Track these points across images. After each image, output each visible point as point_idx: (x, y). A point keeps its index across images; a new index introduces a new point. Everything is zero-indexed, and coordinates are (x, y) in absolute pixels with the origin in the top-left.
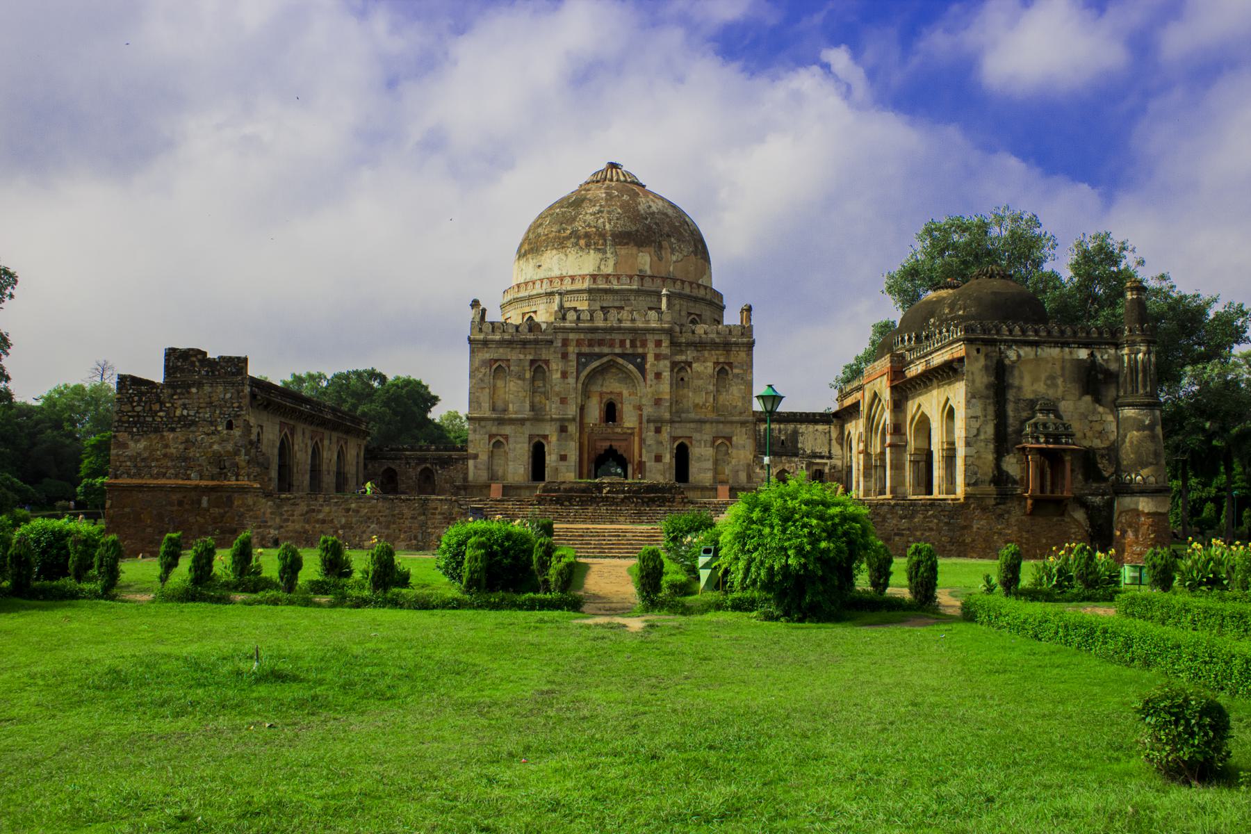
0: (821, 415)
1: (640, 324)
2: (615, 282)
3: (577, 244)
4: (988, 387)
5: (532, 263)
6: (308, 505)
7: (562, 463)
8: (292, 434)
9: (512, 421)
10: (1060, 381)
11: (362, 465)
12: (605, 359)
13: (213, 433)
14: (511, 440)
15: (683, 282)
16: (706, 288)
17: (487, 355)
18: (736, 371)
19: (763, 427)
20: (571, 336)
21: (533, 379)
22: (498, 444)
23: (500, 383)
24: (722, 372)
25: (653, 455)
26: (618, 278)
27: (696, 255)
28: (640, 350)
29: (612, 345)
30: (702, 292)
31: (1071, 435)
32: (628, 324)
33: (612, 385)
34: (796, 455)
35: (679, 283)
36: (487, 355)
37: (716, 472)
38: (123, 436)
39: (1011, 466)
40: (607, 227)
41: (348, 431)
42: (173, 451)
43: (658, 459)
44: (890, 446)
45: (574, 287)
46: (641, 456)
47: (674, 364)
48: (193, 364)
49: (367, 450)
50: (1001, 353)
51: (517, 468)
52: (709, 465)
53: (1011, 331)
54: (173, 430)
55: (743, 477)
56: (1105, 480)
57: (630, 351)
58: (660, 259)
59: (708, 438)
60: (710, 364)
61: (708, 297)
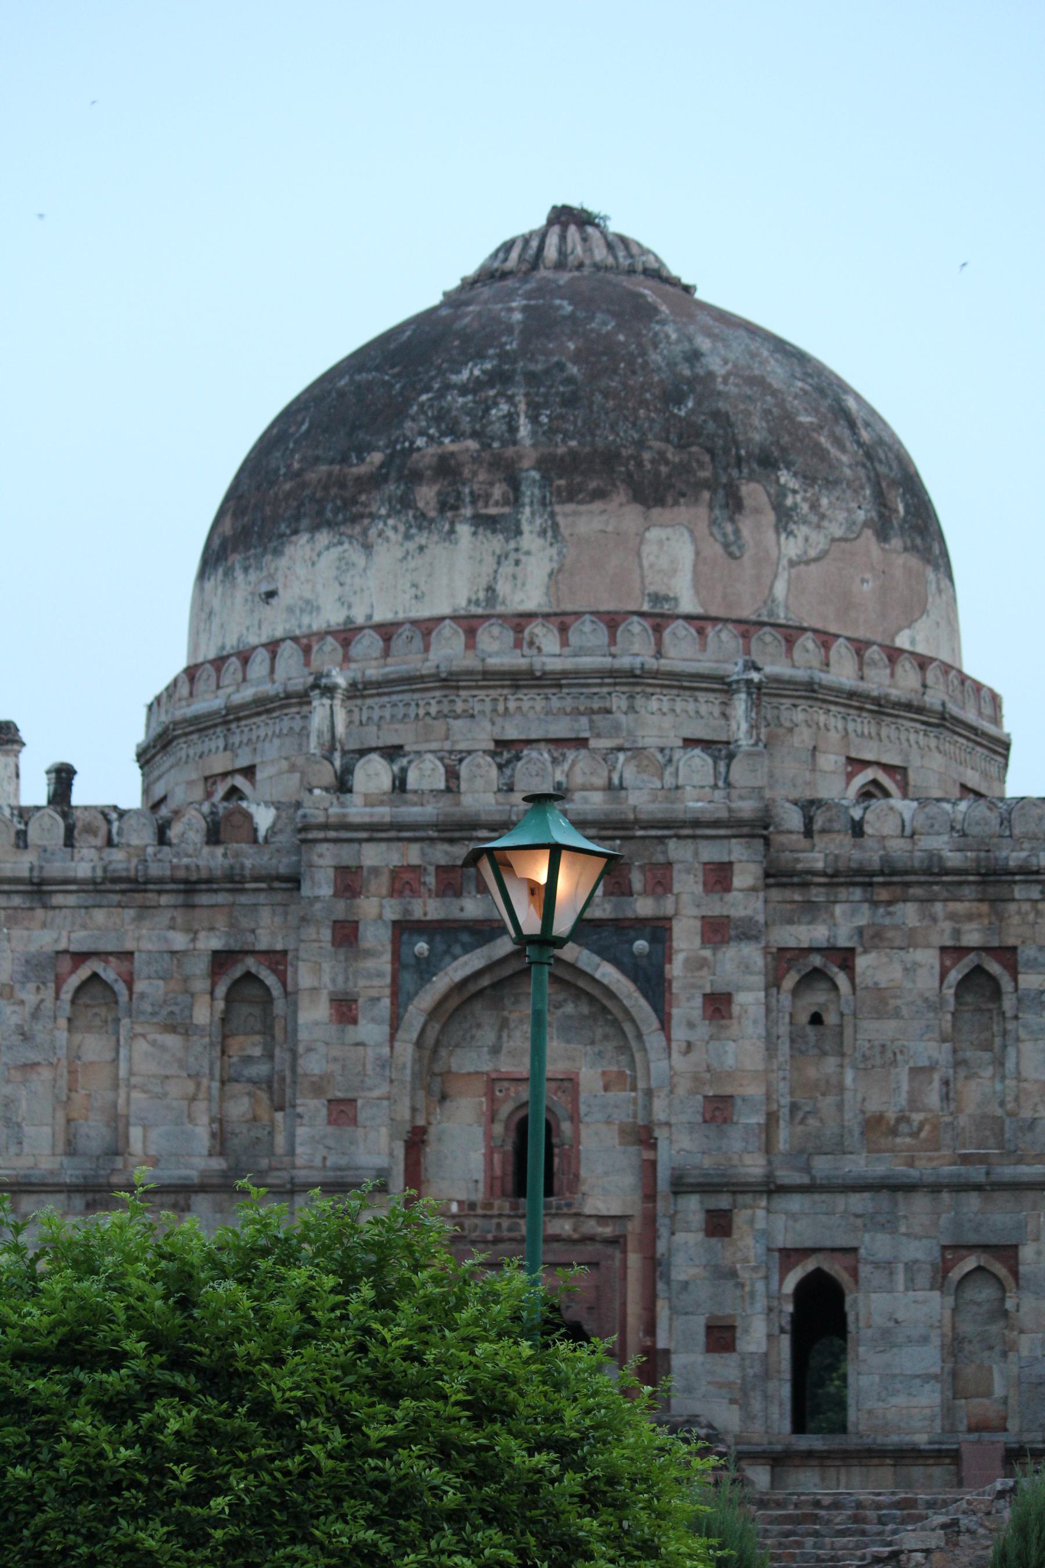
1: (641, 798)
3: (406, 502)
15: (826, 639)
16: (923, 663)
18: (1029, 981)
20: (372, 855)
23: (94, 1046)
25: (698, 1324)
26: (562, 622)
27: (883, 534)
28: (644, 907)
30: (905, 683)
35: (807, 641)
37: (956, 1384)
40: (524, 430)
43: (721, 1337)
45: (395, 667)
46: (650, 1328)
47: (782, 959)
52: (928, 1358)
58: (732, 549)
59: (920, 1251)
60: (928, 958)
61: (933, 699)
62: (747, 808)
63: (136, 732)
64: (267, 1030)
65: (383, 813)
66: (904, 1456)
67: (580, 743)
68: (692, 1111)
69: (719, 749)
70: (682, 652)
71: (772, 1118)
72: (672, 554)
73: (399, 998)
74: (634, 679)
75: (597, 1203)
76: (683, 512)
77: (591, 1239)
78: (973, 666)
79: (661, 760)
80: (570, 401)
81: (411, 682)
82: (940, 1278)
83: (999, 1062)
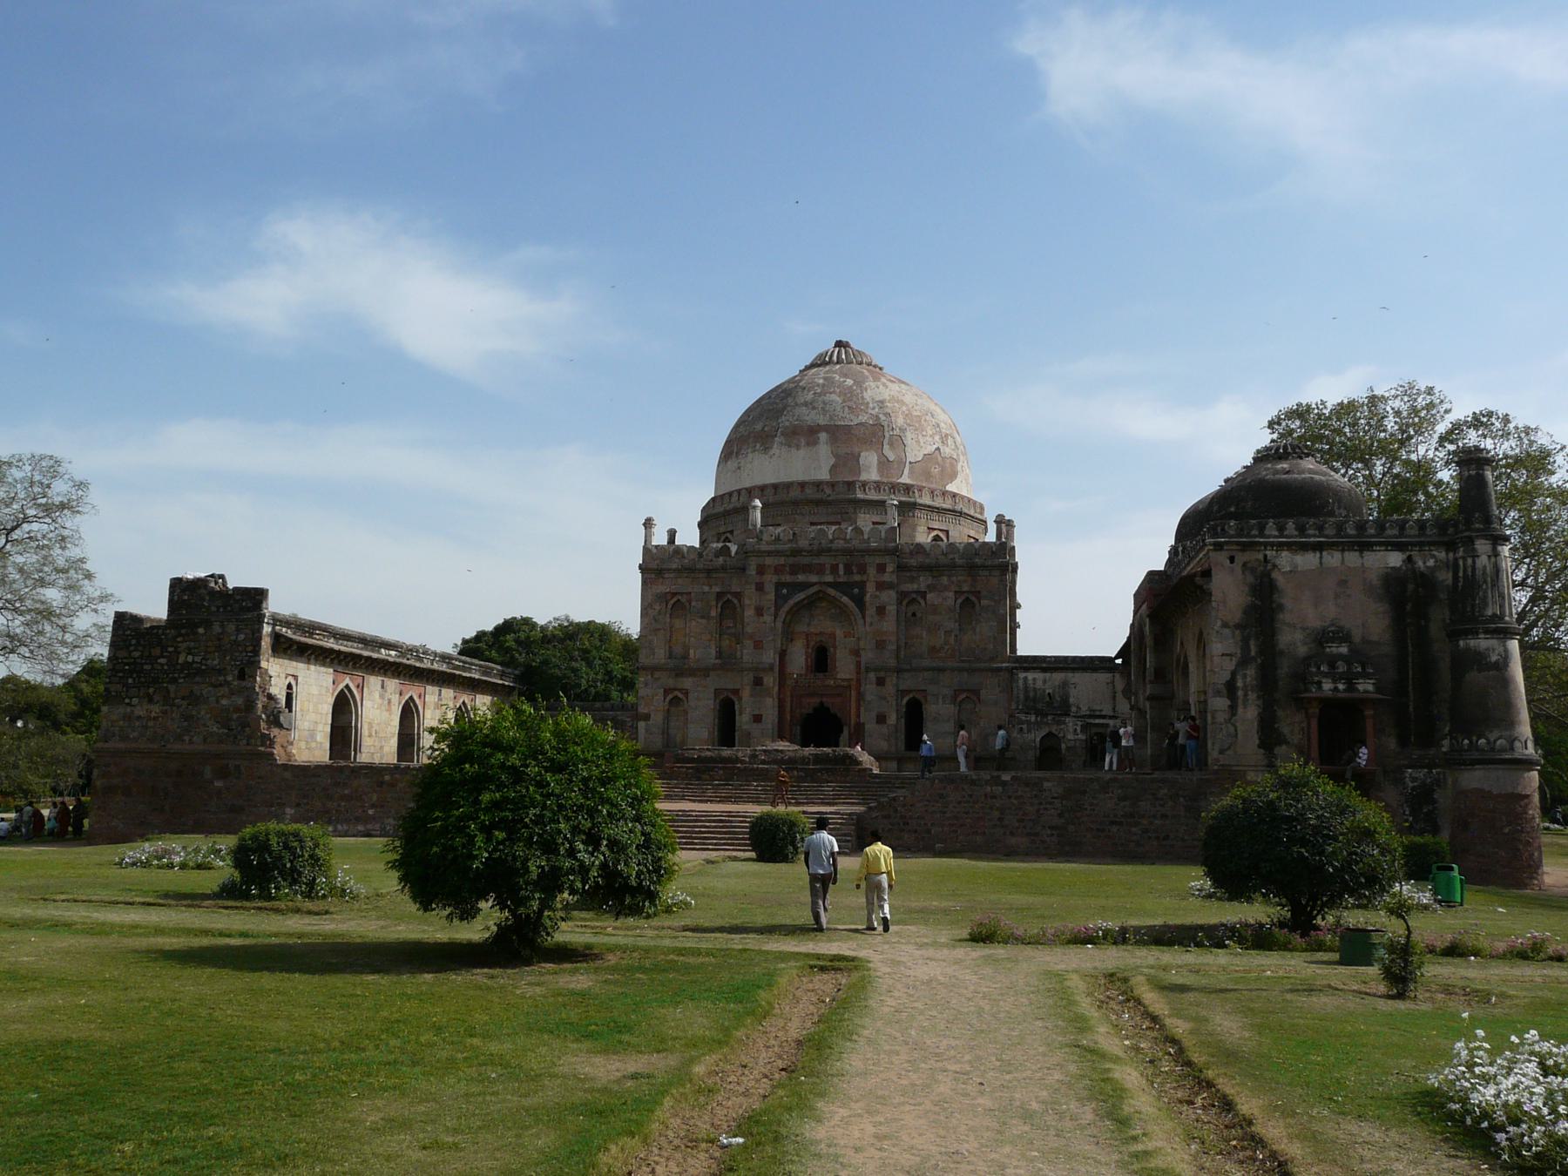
2: (828, 491)
8: (361, 687)
9: (692, 672)
16: (954, 495)
17: (662, 588)
18: (984, 602)
19: (1022, 675)
20: (769, 561)
22: (675, 701)
23: (678, 623)
24: (968, 606)
25: (874, 715)
28: (857, 578)
29: (820, 570)
32: (840, 544)
33: (822, 624)
43: (881, 719)
44: (1151, 698)
47: (903, 595)
53: (1281, 529)
54: (174, 681)
60: (951, 594)
61: (958, 508)
65: (772, 548)
70: (872, 496)
71: (898, 648)
73: (777, 608)
75: (841, 675)
81: (783, 503)
82: (954, 700)
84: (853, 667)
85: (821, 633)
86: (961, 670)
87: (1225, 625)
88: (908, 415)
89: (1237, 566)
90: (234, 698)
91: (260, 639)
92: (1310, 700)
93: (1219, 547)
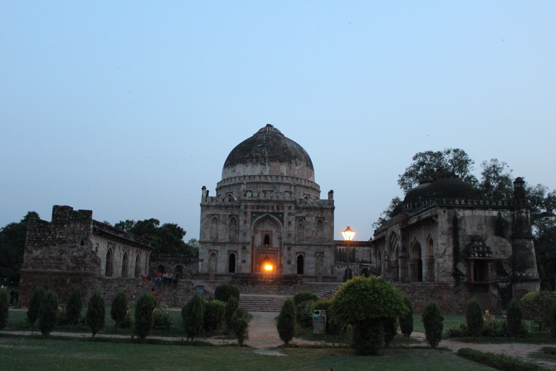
0: (366, 242)
1: (281, 198)
2: (269, 179)
3: (251, 161)
4: (449, 229)
5: (231, 170)
6: (119, 283)
7: (244, 264)
8: (114, 248)
9: (220, 244)
10: (484, 226)
11: (148, 263)
12: (264, 215)
13: (74, 247)
14: (219, 253)
15: (301, 179)
16: (312, 182)
17: (209, 212)
18: (326, 221)
19: (338, 248)
20: (249, 204)
21: (231, 224)
22: (213, 254)
23: (215, 226)
24: (320, 222)
25: (286, 261)
26: (271, 176)
28: (281, 211)
30: (310, 184)
31: (491, 253)
32: (275, 199)
33: (267, 227)
34: (354, 261)
36: (209, 212)
37: (316, 268)
38: (29, 248)
39: (462, 267)
41: (142, 247)
42: (54, 255)
43: (289, 262)
44: (401, 257)
47: (297, 218)
48: (66, 213)
49: (151, 257)
50: (455, 213)
51: (222, 266)
52: (314, 266)
53: (460, 202)
54: (55, 245)
55: (329, 271)
56: (508, 275)
57: (276, 211)
58: (290, 168)
59: (313, 253)
60: (314, 218)
61: (313, 186)
62: (293, 200)
63: (216, 187)
64: (235, 225)
65: (250, 199)
66: (310, 277)
67: (273, 191)
68: (286, 236)
69: (290, 193)
70: (285, 181)
72: (284, 169)
74: (279, 184)
76: (285, 164)
77: (273, 250)
78: (317, 181)
79: (282, 194)
80: (271, 149)
81: (253, 183)
82: (315, 256)
83: (322, 231)
84: (278, 243)
85: (267, 231)
86: (317, 245)
87: (443, 234)
88: (296, 153)
89: (446, 214)
90: (79, 252)
91: (90, 229)
92: (471, 259)
93: (441, 207)
